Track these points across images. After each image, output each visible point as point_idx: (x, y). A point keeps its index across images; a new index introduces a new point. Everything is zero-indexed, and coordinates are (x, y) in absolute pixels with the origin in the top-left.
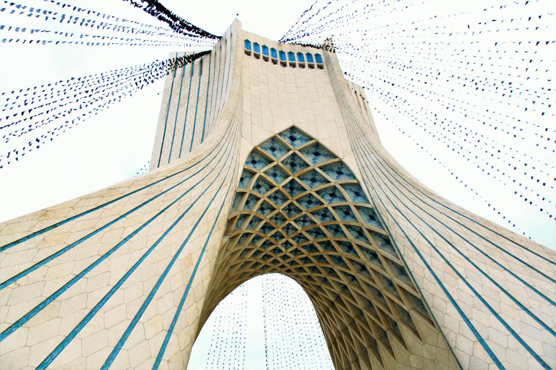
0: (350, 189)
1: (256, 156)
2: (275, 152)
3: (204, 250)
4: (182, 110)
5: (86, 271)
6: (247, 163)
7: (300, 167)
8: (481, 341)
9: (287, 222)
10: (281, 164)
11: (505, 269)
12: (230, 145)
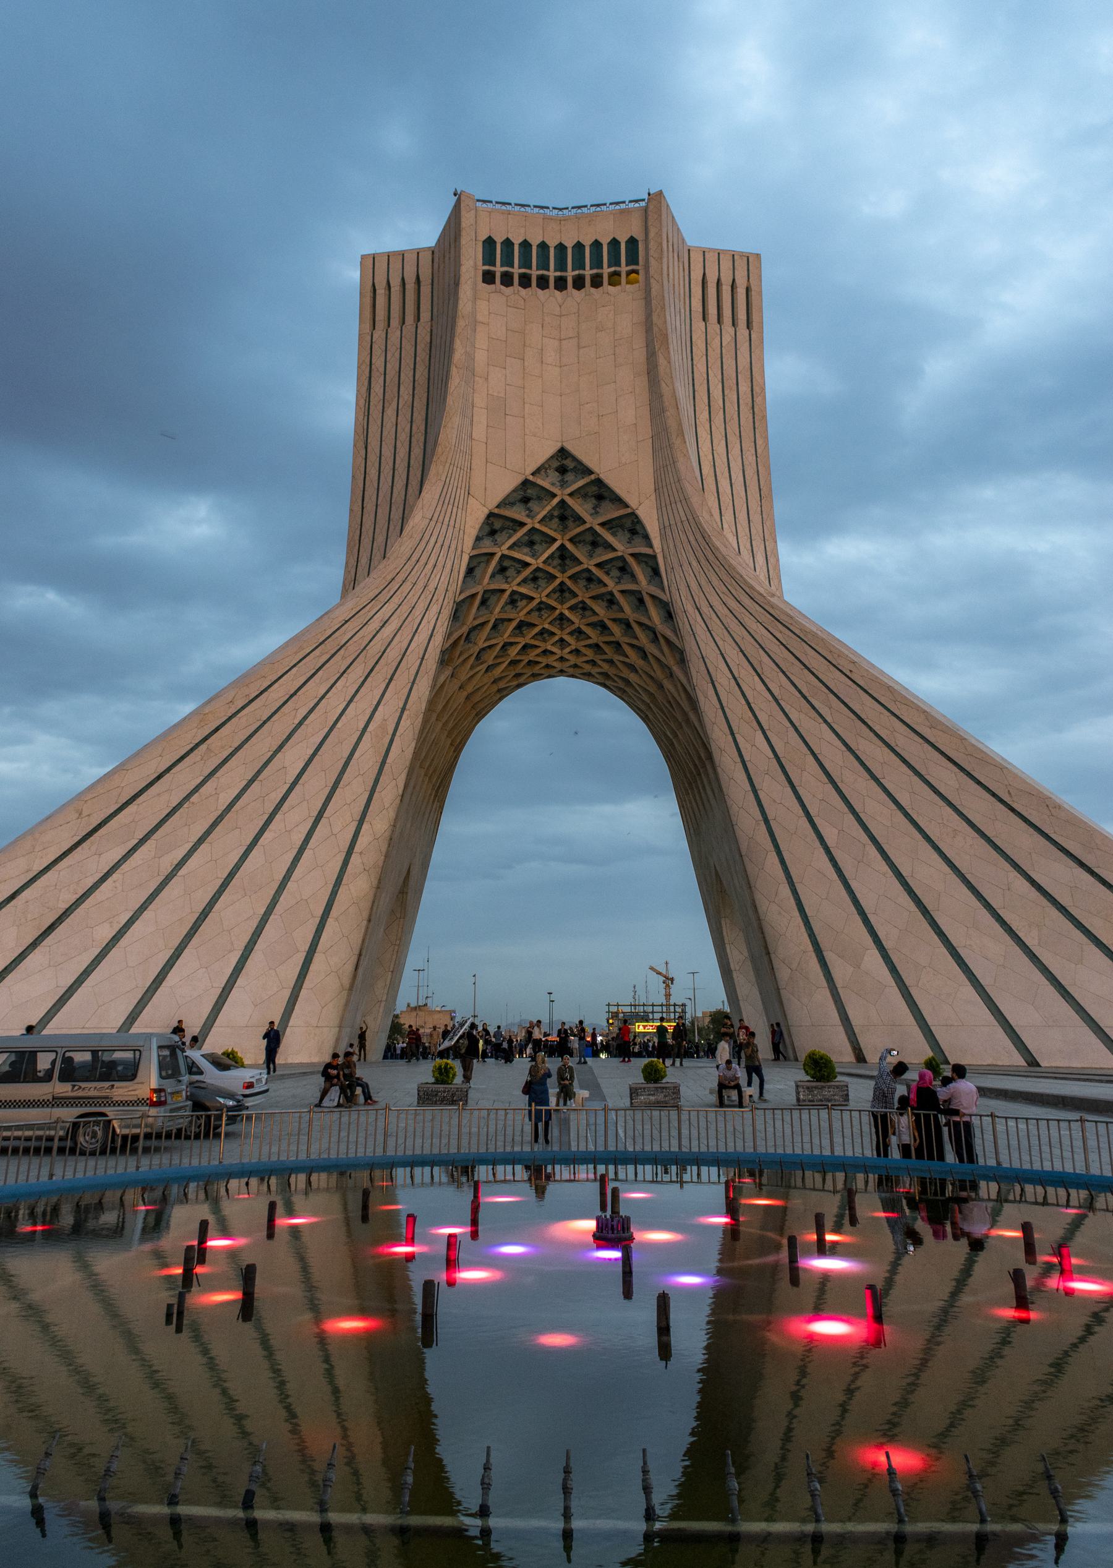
0: (646, 563)
1: (495, 525)
2: (530, 504)
3: (403, 709)
4: (390, 412)
5: (259, 772)
6: (478, 539)
7: (574, 521)
8: (766, 820)
9: (557, 612)
10: (537, 526)
11: (825, 721)
12: (445, 527)
